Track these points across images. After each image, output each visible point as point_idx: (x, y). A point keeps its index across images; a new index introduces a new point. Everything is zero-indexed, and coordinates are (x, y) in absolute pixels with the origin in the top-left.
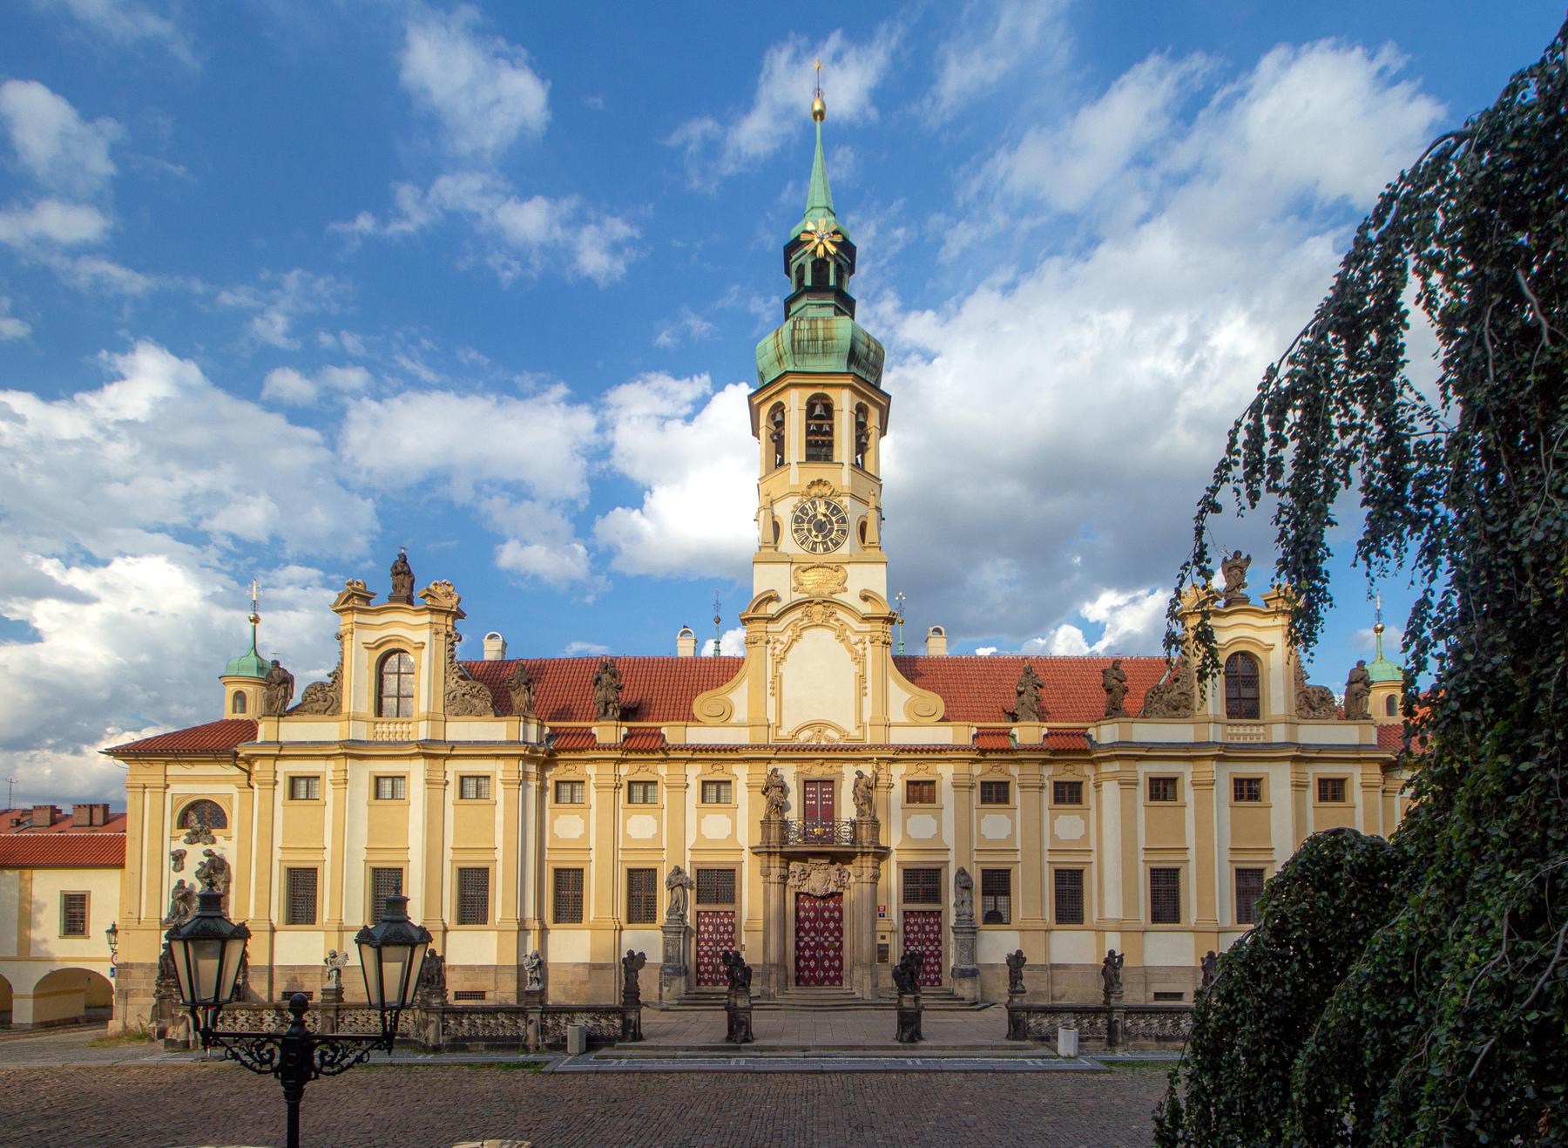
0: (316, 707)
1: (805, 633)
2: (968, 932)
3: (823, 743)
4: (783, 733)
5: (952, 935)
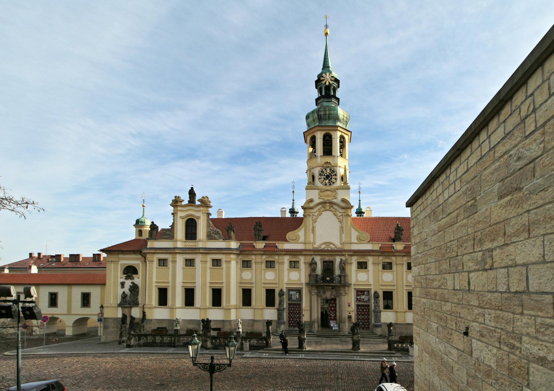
0: (164, 237)
2: (378, 313)
3: (329, 249)
4: (316, 246)
5: (373, 313)
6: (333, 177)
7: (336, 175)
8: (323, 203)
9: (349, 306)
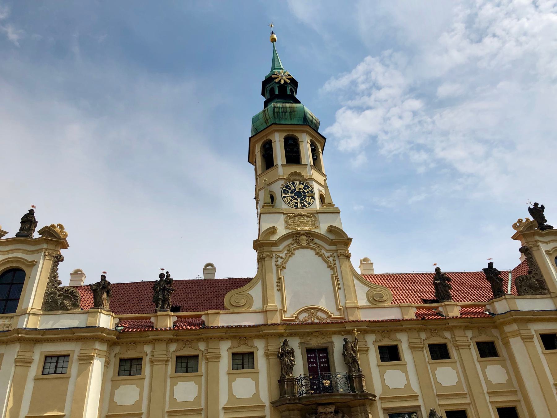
1: (296, 252)
3: (316, 321)
6: (307, 195)
7: (312, 192)
8: (295, 236)
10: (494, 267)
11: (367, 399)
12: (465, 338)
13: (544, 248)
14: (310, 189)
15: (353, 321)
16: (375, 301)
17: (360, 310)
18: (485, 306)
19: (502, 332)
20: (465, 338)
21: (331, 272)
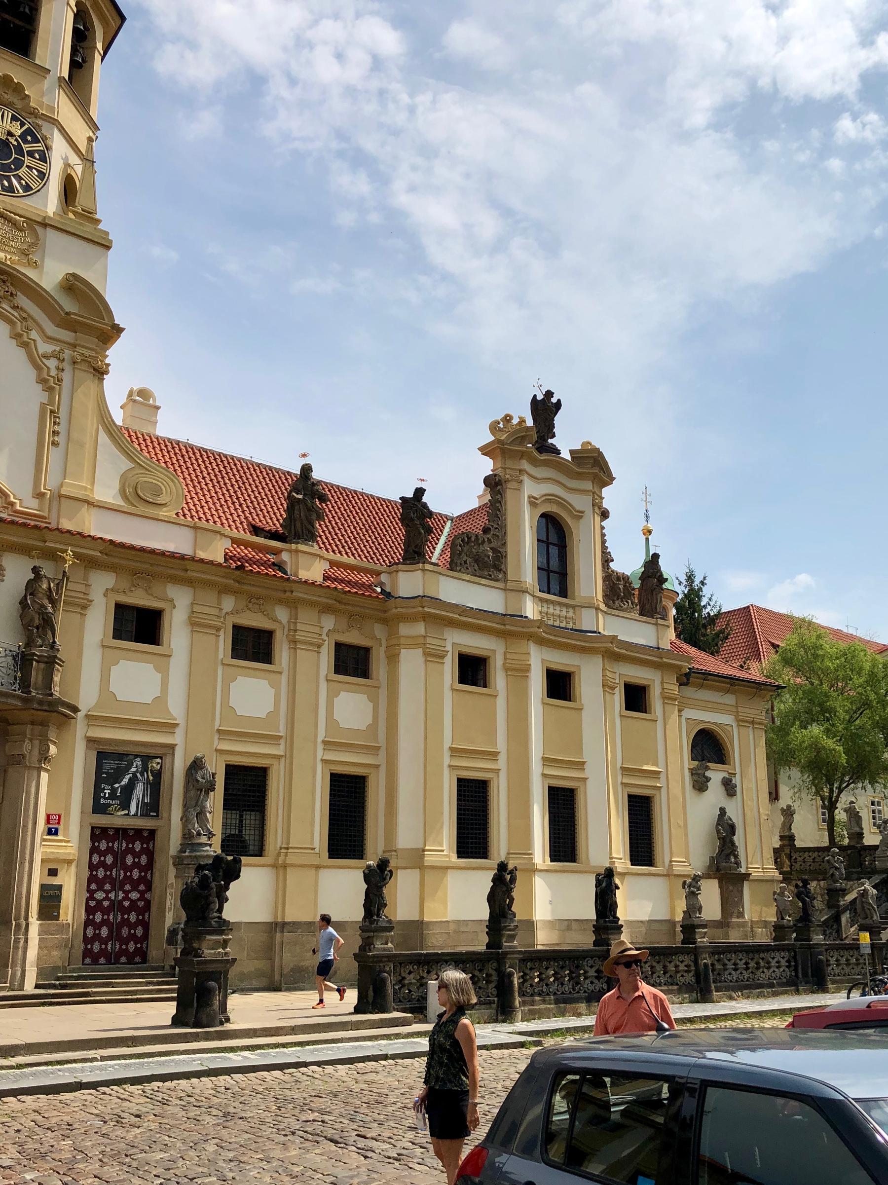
5: (172, 872)
6: (27, 161)
7: (44, 159)
9: (52, 832)
10: (424, 499)
11: (56, 712)
12: (317, 630)
13: (530, 488)
14: (40, 147)
15: (69, 532)
16: (138, 499)
17: (94, 511)
18: (378, 574)
19: (392, 633)
20: (317, 630)
21: (44, 397)
